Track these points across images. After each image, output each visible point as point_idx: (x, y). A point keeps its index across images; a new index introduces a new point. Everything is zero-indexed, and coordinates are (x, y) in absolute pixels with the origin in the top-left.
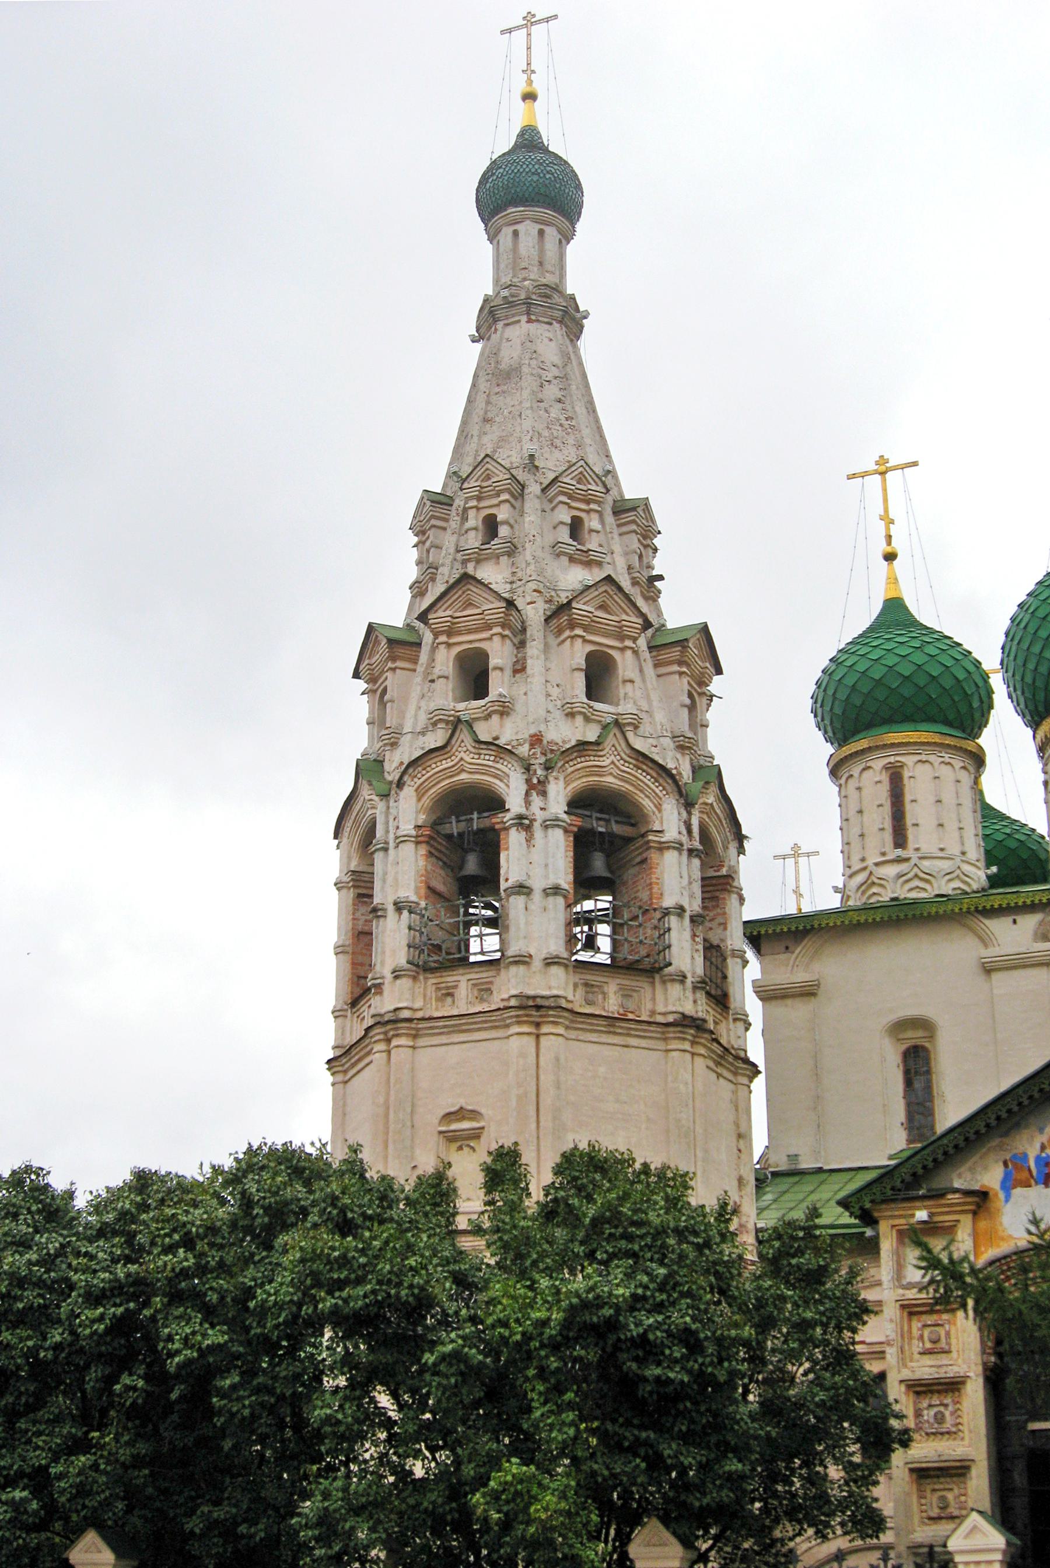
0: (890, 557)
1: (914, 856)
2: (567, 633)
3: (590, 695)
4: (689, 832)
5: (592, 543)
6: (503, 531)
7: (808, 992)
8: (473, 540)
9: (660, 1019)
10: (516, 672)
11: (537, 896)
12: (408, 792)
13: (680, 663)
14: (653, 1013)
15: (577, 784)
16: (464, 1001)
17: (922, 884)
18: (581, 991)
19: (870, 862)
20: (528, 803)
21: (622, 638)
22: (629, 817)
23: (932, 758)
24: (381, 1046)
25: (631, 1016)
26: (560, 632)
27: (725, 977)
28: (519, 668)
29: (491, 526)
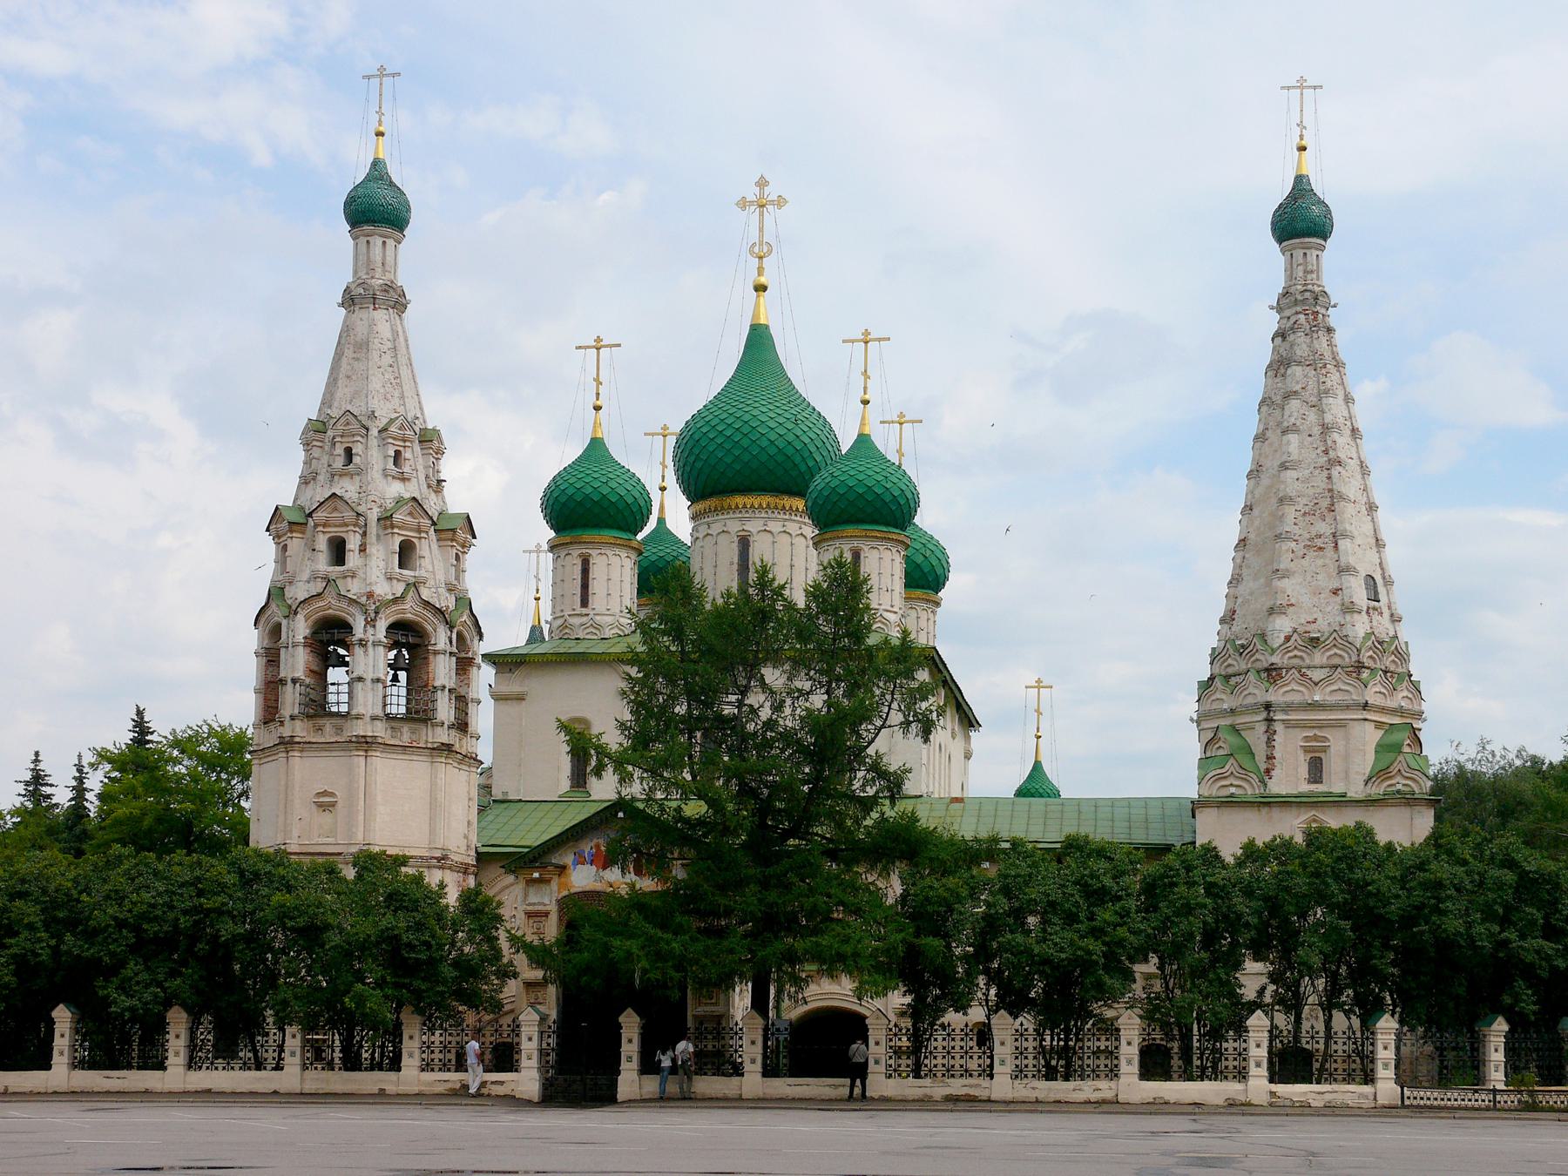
0: (597, 408)
1: (592, 613)
2: (390, 531)
3: (401, 566)
4: (451, 642)
5: (406, 469)
6: (356, 460)
7: (520, 698)
8: (339, 463)
9: (429, 745)
10: (360, 551)
11: (368, 682)
12: (300, 617)
13: (452, 540)
14: (427, 742)
15: (391, 620)
16: (329, 735)
17: (594, 631)
18: (389, 731)
19: (566, 614)
20: (365, 631)
21: (419, 531)
22: (419, 632)
23: (608, 552)
24: (284, 755)
25: (415, 744)
26: (386, 528)
27: (467, 714)
28: (363, 549)
29: (349, 453)
